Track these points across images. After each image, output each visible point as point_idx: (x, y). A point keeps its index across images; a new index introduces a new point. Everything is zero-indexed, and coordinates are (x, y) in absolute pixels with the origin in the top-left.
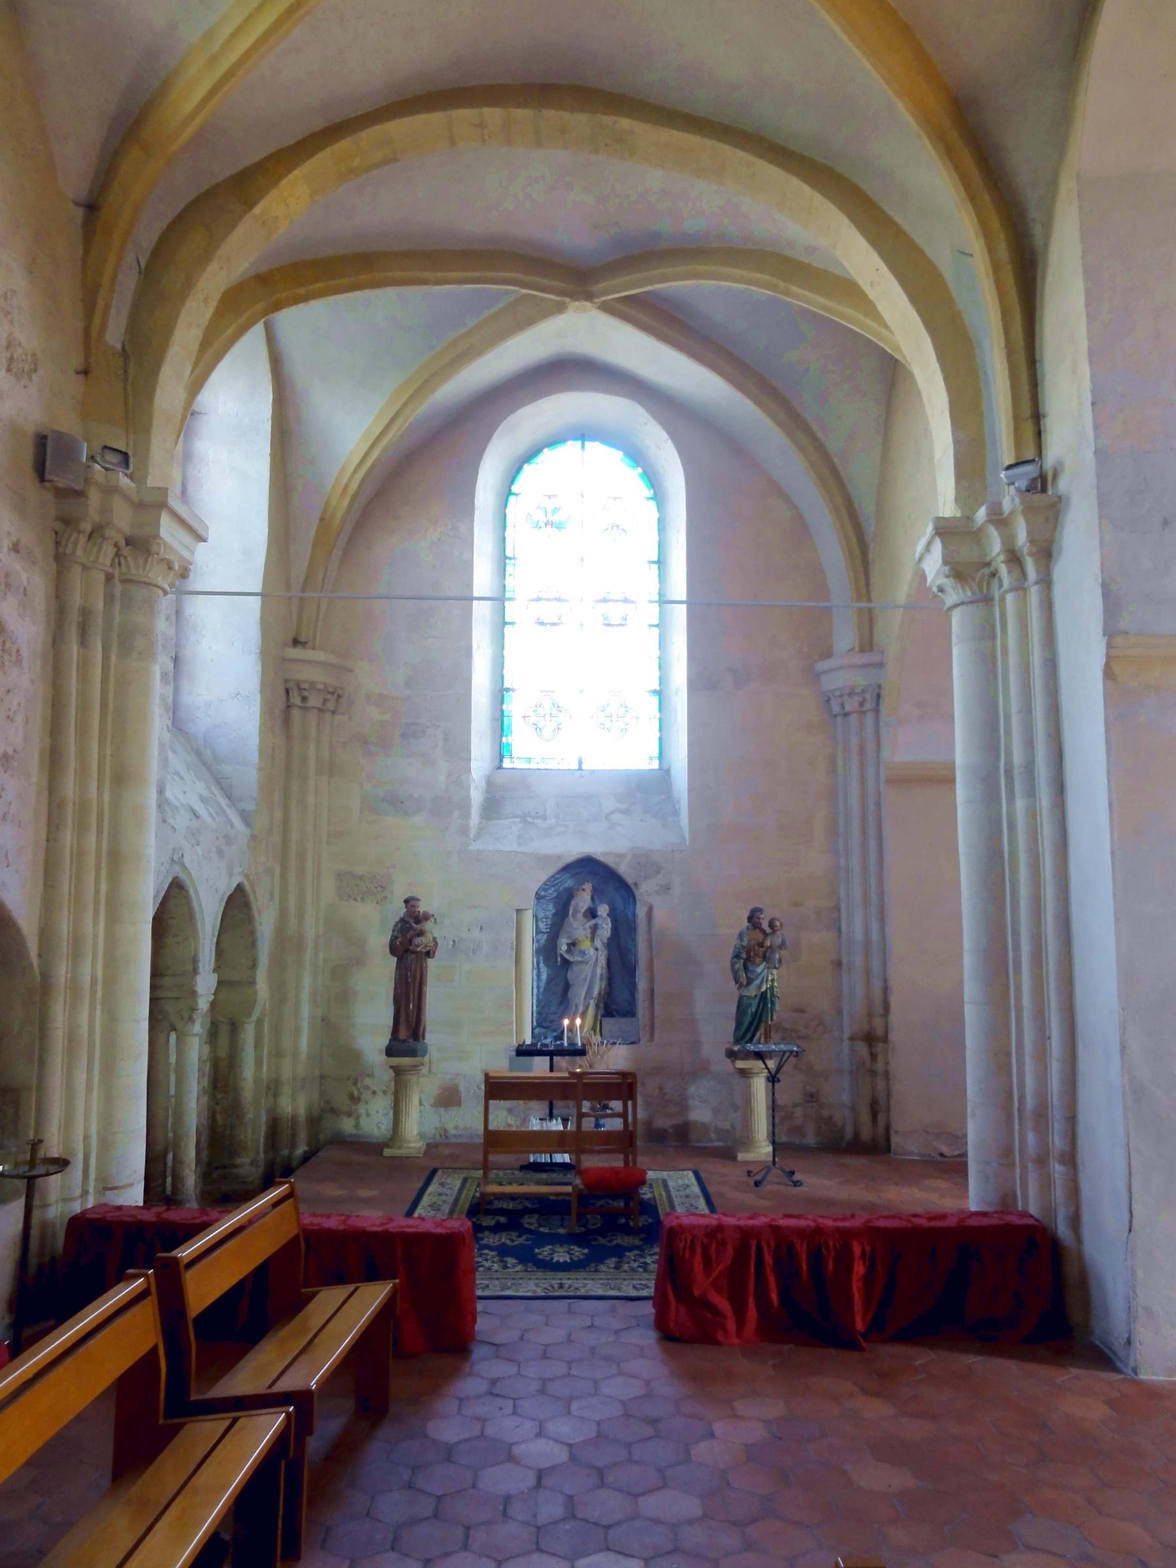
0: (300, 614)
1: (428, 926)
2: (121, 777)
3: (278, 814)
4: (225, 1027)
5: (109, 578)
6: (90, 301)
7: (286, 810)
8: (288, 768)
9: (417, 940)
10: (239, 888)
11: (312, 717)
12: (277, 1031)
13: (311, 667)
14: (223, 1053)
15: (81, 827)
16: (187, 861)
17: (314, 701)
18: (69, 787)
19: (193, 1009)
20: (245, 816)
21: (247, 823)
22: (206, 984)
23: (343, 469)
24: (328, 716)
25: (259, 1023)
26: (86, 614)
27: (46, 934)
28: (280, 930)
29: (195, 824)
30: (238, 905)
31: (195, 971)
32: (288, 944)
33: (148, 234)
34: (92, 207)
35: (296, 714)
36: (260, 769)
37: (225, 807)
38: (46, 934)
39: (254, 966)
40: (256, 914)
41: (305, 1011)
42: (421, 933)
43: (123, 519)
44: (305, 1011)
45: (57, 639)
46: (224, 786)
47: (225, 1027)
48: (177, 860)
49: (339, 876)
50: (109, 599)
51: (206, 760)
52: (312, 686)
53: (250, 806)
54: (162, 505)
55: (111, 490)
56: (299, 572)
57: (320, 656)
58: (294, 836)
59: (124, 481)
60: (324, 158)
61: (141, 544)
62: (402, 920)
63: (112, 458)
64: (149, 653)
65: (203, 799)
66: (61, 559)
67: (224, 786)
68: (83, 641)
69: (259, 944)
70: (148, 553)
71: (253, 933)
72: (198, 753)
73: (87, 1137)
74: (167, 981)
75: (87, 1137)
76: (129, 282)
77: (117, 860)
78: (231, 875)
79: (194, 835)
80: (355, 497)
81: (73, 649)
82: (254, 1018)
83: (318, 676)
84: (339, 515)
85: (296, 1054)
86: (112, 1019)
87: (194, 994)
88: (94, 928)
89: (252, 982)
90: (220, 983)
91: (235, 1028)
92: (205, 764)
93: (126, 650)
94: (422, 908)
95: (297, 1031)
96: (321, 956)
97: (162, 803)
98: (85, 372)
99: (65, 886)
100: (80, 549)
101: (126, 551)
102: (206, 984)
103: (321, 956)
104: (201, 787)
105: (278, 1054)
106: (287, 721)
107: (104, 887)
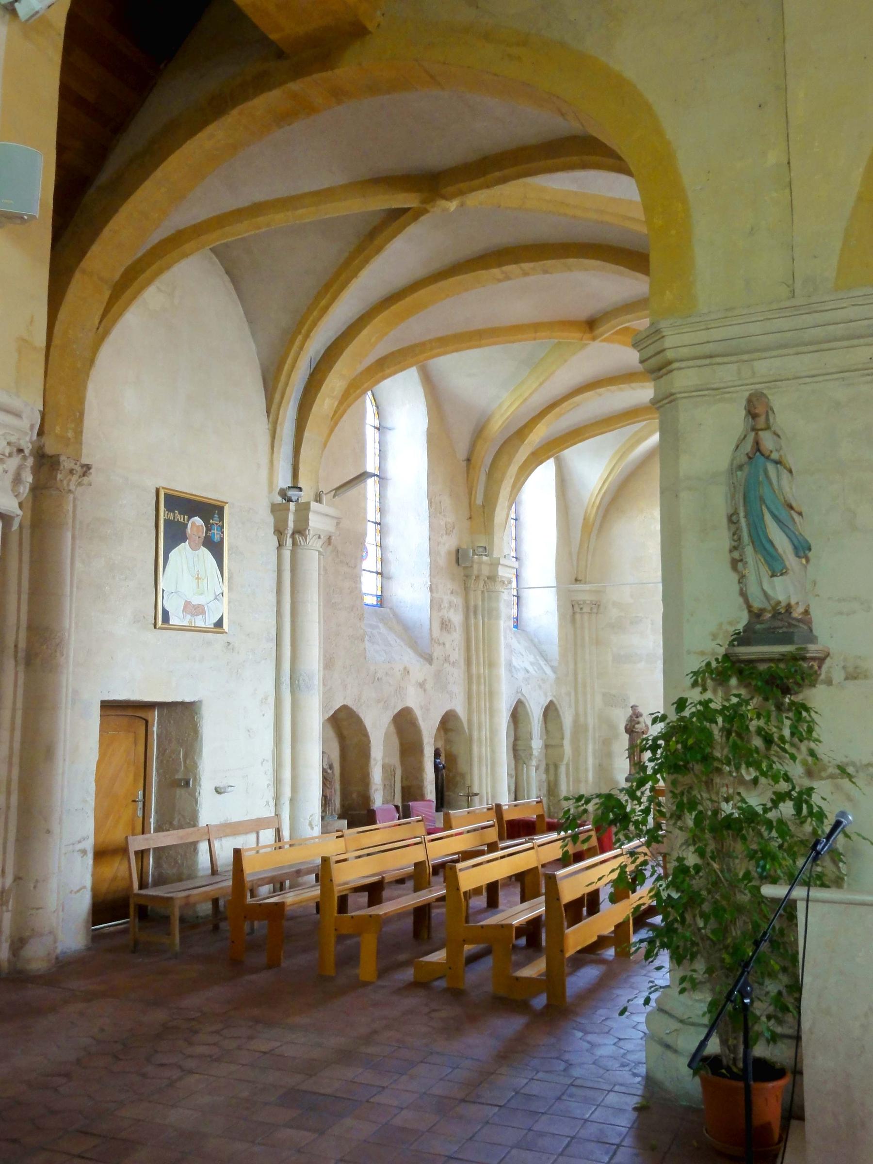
0: (578, 566)
1: (641, 719)
2: (491, 664)
3: (571, 666)
4: (552, 767)
5: (483, 592)
7: (576, 664)
8: (576, 644)
9: (637, 726)
10: (551, 702)
11: (586, 617)
12: (577, 769)
13: (584, 593)
14: (552, 778)
15: (479, 684)
16: (524, 692)
17: (586, 609)
19: (531, 755)
21: (555, 672)
22: (537, 745)
23: (592, 495)
24: (594, 616)
25: (567, 765)
26: (476, 607)
27: (470, 721)
28: (576, 722)
29: (527, 675)
30: (550, 711)
31: (531, 739)
32: (579, 728)
33: (488, 461)
34: (468, 460)
35: (578, 616)
36: (560, 646)
37: (544, 666)
38: (470, 721)
39: (563, 738)
40: (561, 713)
41: (590, 761)
42: (638, 723)
43: (485, 571)
44: (590, 761)
45: (467, 618)
46: (543, 655)
48: (519, 691)
49: (604, 695)
50: (483, 600)
51: (536, 645)
52: (584, 602)
53: (555, 664)
54: (499, 564)
55: (480, 563)
57: (587, 587)
58: (580, 676)
59: (484, 558)
60: (549, 416)
61: (492, 578)
62: (631, 717)
63: (481, 550)
64: (498, 617)
65: (532, 664)
66: (466, 589)
67: (543, 655)
68: (475, 617)
69: (564, 728)
70: (495, 581)
71: (561, 723)
72: (532, 641)
73: (487, 793)
74: (519, 743)
75: (487, 793)
76: (483, 478)
77: (491, 695)
78: (546, 696)
79: (527, 680)
80: (598, 508)
81: (473, 621)
82: (565, 763)
83: (587, 597)
84: (592, 516)
85: (586, 781)
87: (531, 748)
88: (485, 718)
89: (562, 746)
90: (547, 746)
91: (556, 767)
92: (535, 646)
93: (490, 618)
94: (640, 710)
95: (586, 770)
96: (597, 735)
98: (470, 518)
99: (474, 705)
100: (472, 583)
101: (488, 581)
102: (537, 745)
103: (597, 735)
104: (531, 658)
105: (577, 781)
106: (573, 621)
107: (487, 704)
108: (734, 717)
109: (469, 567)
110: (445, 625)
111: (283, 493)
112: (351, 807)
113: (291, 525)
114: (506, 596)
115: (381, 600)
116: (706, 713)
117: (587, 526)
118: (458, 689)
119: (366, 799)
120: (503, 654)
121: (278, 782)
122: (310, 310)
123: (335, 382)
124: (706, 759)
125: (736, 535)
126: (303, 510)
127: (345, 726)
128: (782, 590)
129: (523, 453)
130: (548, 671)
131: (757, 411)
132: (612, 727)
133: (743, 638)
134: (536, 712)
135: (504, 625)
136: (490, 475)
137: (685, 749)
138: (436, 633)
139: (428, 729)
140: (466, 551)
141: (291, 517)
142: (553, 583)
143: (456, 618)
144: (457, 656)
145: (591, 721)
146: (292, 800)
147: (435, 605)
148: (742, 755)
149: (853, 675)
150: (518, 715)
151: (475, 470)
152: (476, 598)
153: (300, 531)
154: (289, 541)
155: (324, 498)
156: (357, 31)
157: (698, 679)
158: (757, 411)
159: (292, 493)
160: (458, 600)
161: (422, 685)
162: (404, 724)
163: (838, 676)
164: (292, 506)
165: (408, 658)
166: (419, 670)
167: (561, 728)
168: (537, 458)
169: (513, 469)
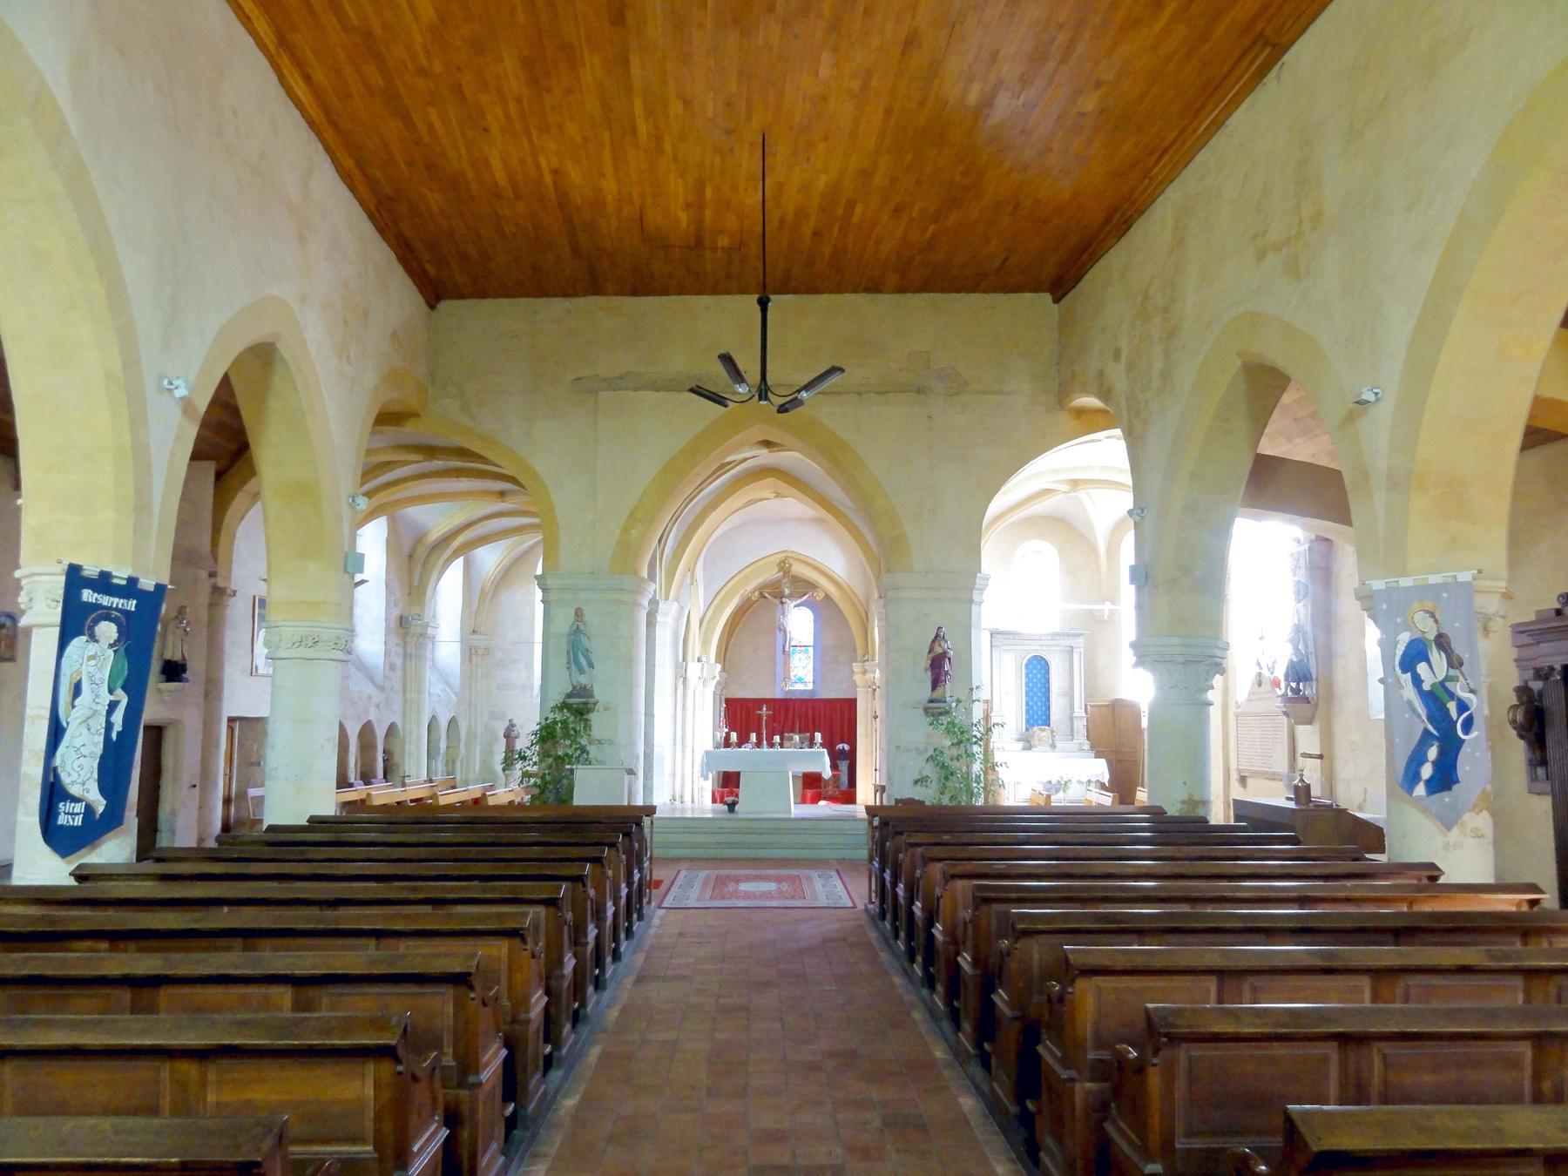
2: (420, 692)
6: (410, 577)
22: (443, 745)
30: (453, 722)
32: (471, 736)
34: (410, 556)
46: (448, 684)
47: (450, 762)
51: (444, 678)
61: (423, 635)
67: (448, 684)
77: (419, 711)
86: (418, 749)
102: (443, 745)
108: (564, 722)
109: (408, 627)
110: (392, 667)
116: (555, 722)
117: (483, 593)
118: (397, 708)
128: (583, 680)
131: (579, 614)
133: (569, 696)
135: (428, 664)
142: (458, 638)
143: (398, 661)
144: (398, 686)
147: (387, 654)
148: (567, 736)
149: (606, 709)
150: (432, 725)
151: (415, 564)
157: (553, 710)
158: (579, 614)
165: (370, 689)
166: (378, 697)
168: (455, 555)
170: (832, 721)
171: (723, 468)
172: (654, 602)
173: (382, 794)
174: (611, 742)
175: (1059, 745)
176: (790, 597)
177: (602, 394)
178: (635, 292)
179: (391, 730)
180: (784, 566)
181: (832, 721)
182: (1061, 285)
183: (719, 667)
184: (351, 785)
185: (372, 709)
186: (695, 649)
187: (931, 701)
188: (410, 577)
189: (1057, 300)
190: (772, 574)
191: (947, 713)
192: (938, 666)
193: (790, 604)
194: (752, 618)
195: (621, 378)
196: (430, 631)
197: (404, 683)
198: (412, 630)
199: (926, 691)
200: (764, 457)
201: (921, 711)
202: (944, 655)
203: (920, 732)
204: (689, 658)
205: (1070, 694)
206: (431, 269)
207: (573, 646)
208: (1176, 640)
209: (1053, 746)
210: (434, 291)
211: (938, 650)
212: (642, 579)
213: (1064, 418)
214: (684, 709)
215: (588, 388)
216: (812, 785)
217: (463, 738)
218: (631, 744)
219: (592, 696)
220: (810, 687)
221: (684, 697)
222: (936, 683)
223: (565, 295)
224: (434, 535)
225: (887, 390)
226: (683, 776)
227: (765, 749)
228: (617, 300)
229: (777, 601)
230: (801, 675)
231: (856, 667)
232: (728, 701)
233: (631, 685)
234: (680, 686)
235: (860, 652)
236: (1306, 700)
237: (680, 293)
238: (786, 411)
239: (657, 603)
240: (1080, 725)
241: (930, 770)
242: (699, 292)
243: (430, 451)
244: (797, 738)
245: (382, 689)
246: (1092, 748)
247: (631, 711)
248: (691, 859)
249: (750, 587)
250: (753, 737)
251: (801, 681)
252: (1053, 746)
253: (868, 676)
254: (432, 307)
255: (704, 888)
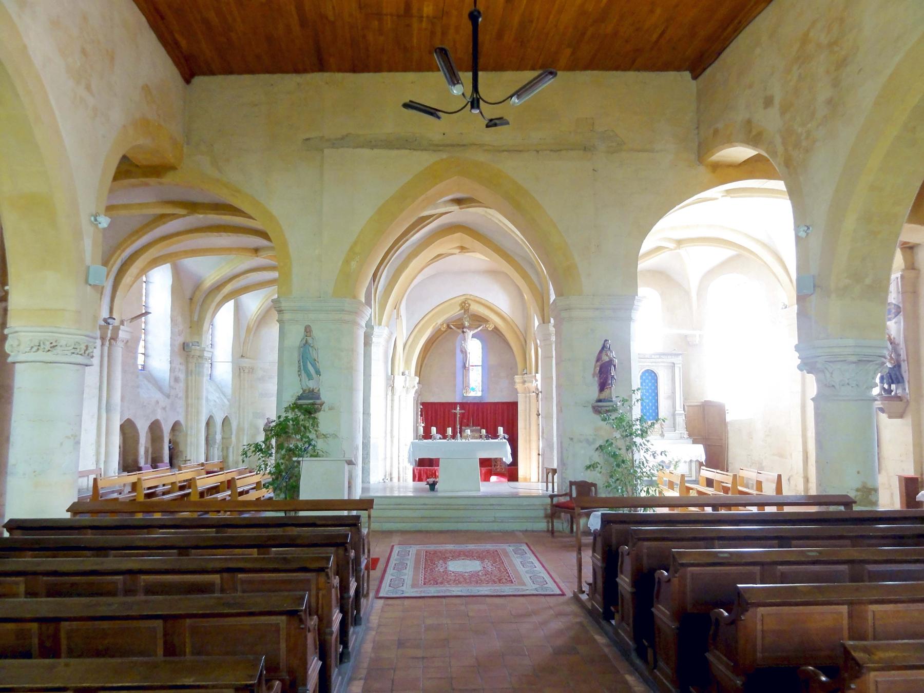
2: (198, 398)
6: (191, 316)
13: (246, 363)
17: (246, 371)
18: (190, 401)
20: (228, 400)
22: (218, 437)
30: (226, 421)
32: (240, 429)
34: (191, 299)
46: (224, 394)
51: (220, 389)
56: (242, 340)
66: (187, 362)
76: (198, 308)
77: (198, 413)
90: (223, 438)
91: (227, 448)
97: (207, 400)
102: (218, 437)
108: (295, 420)
109: (189, 351)
110: (177, 380)
111: (105, 320)
112: (129, 464)
113: (109, 335)
114: (207, 365)
115: (144, 366)
117: (249, 330)
119: (136, 461)
120: (204, 394)
121: (98, 454)
122: (125, 240)
123: (133, 270)
124: (286, 433)
125: (299, 367)
126: (116, 330)
127: (128, 430)
128: (311, 384)
129: (219, 297)
130: (225, 401)
131: (308, 330)
132: (257, 429)
133: (299, 398)
134: (219, 421)
135: (206, 379)
136: (201, 306)
137: (280, 430)
138: (172, 384)
139: (166, 429)
140: (188, 345)
141: (109, 332)
142: (230, 359)
143: (182, 376)
145: (246, 426)
146: (105, 462)
147: (172, 370)
148: (298, 431)
151: (194, 304)
152: (192, 366)
153: (114, 338)
154: (107, 343)
155: (125, 323)
156: (173, 168)
157: (286, 410)
158: (308, 330)
159: (110, 321)
160: (183, 368)
161: (164, 409)
162: (155, 428)
163: (327, 409)
164: (111, 327)
165: (158, 396)
166: (164, 402)
167: (231, 429)
168: (226, 299)
169: (214, 304)
170: (499, 418)
171: (422, 221)
172: (369, 326)
173: (150, 478)
174: (335, 436)
175: (666, 434)
176: (470, 328)
177: (326, 151)
178: (354, 70)
179: (176, 427)
180: (464, 306)
181: (499, 418)
182: (698, 65)
183: (417, 379)
184: (140, 469)
185: (159, 411)
186: (400, 365)
187: (599, 401)
188: (191, 316)
189: (695, 77)
190: (456, 311)
191: (615, 410)
192: (605, 374)
193: (470, 333)
194: (439, 345)
195: (343, 138)
196: (206, 354)
197: (187, 391)
198: (192, 353)
199: (593, 392)
200: (457, 214)
201: (590, 409)
202: (610, 362)
203: (592, 427)
204: (396, 372)
205: (673, 397)
206: (183, 43)
207: (305, 357)
208: (851, 342)
209: (662, 435)
210: (190, 67)
211: (605, 359)
212: (361, 302)
213: (703, 172)
214: (392, 410)
215: (314, 147)
216: (489, 467)
217: (234, 432)
218: (352, 438)
219: (318, 398)
220: (479, 394)
221: (392, 400)
222: (603, 386)
223: (296, 71)
224: (208, 283)
225: (559, 148)
226: (392, 458)
227: (459, 441)
228: (339, 75)
229: (460, 331)
230: (475, 387)
231: (518, 379)
232: (423, 404)
233: (351, 389)
234: (390, 393)
235: (520, 366)
236: (899, 398)
237: (390, 70)
238: (495, 125)
239: (372, 328)
240: (681, 420)
241: (597, 457)
242: (406, 69)
243: (193, 207)
244: (468, 432)
245: (168, 396)
246: (690, 435)
247: (351, 411)
248: (403, 532)
249: (440, 321)
250: (449, 431)
251: (473, 390)
252: (662, 435)
253: (527, 385)
254: (188, 81)
255: (416, 568)
